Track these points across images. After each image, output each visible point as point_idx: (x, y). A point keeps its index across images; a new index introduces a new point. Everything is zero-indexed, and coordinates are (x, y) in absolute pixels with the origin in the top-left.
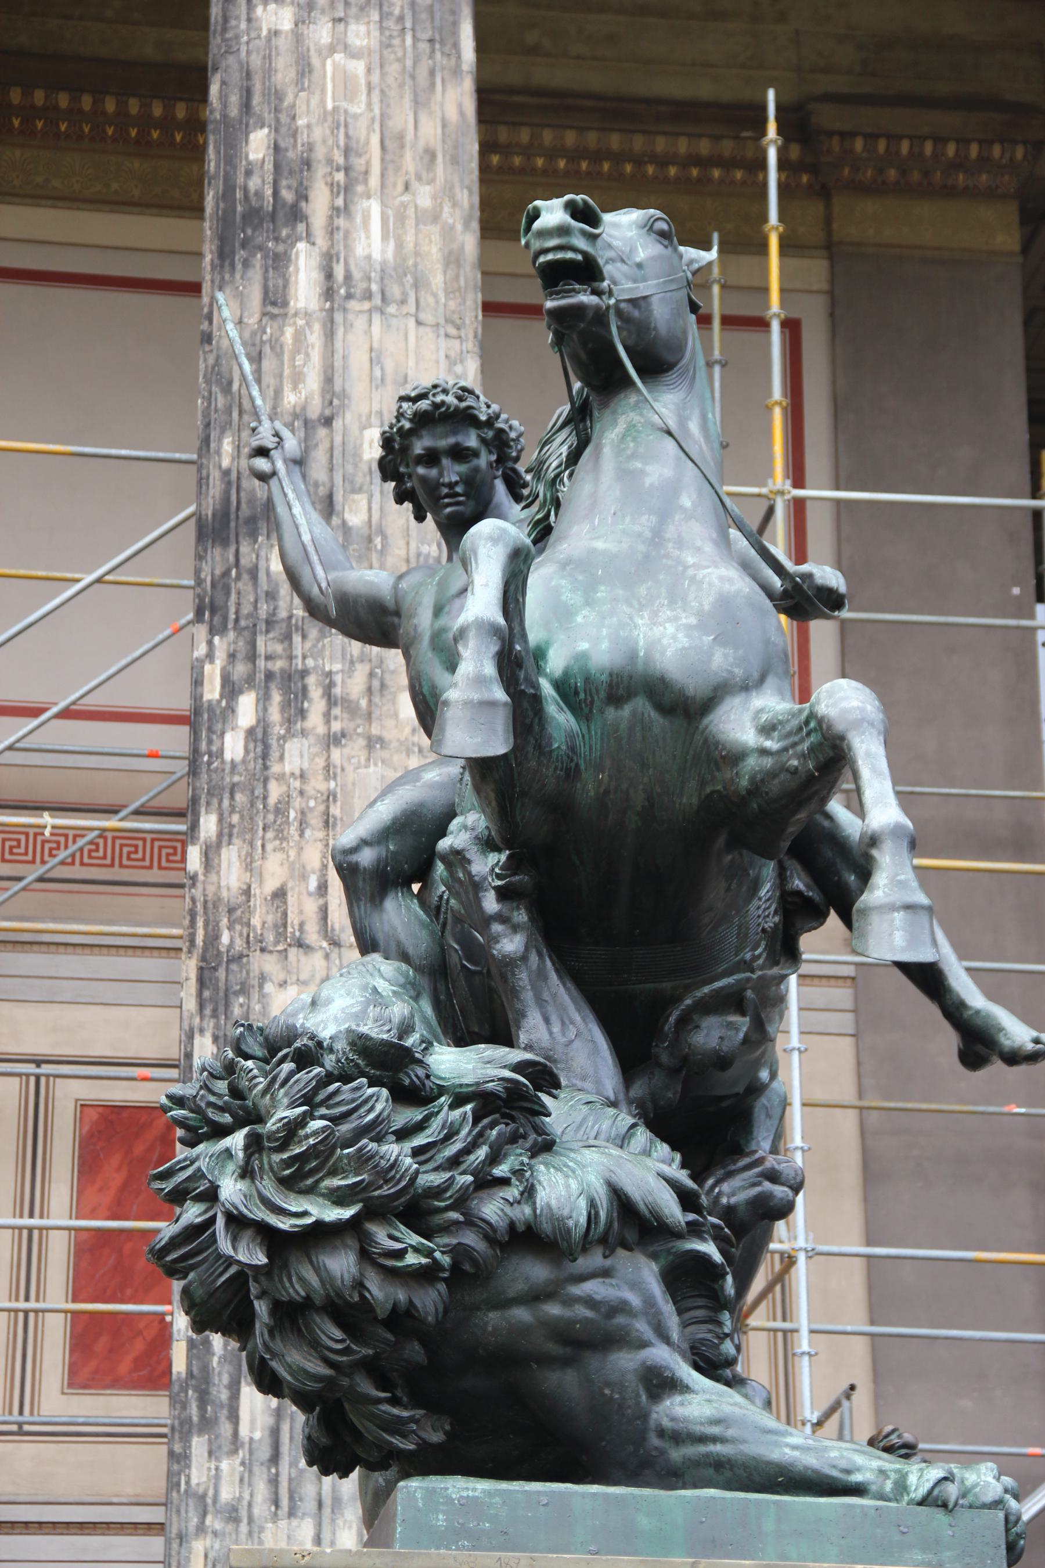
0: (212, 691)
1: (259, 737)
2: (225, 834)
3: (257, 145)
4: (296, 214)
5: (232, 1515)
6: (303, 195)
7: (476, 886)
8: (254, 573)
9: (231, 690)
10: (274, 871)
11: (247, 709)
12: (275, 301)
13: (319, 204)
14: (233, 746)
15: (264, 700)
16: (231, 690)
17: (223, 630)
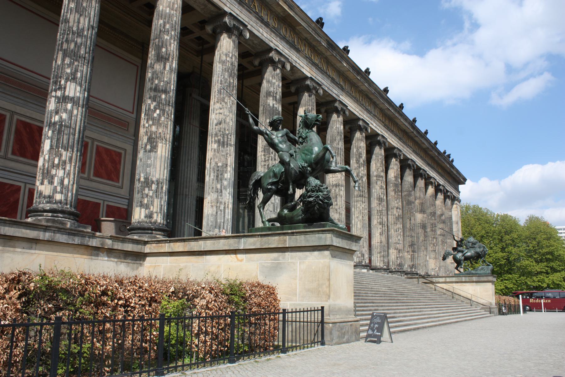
0: (152, 107)
1: (159, 115)
2: (153, 124)
3: (164, 50)
4: (168, 59)
5: (152, 197)
6: (169, 58)
7: (307, 170)
8: (160, 97)
9: (155, 109)
10: (160, 130)
11: (158, 111)
12: (165, 68)
13: (170, 59)
14: (155, 115)
15: (160, 111)
16: (155, 109)
17: (155, 101)
